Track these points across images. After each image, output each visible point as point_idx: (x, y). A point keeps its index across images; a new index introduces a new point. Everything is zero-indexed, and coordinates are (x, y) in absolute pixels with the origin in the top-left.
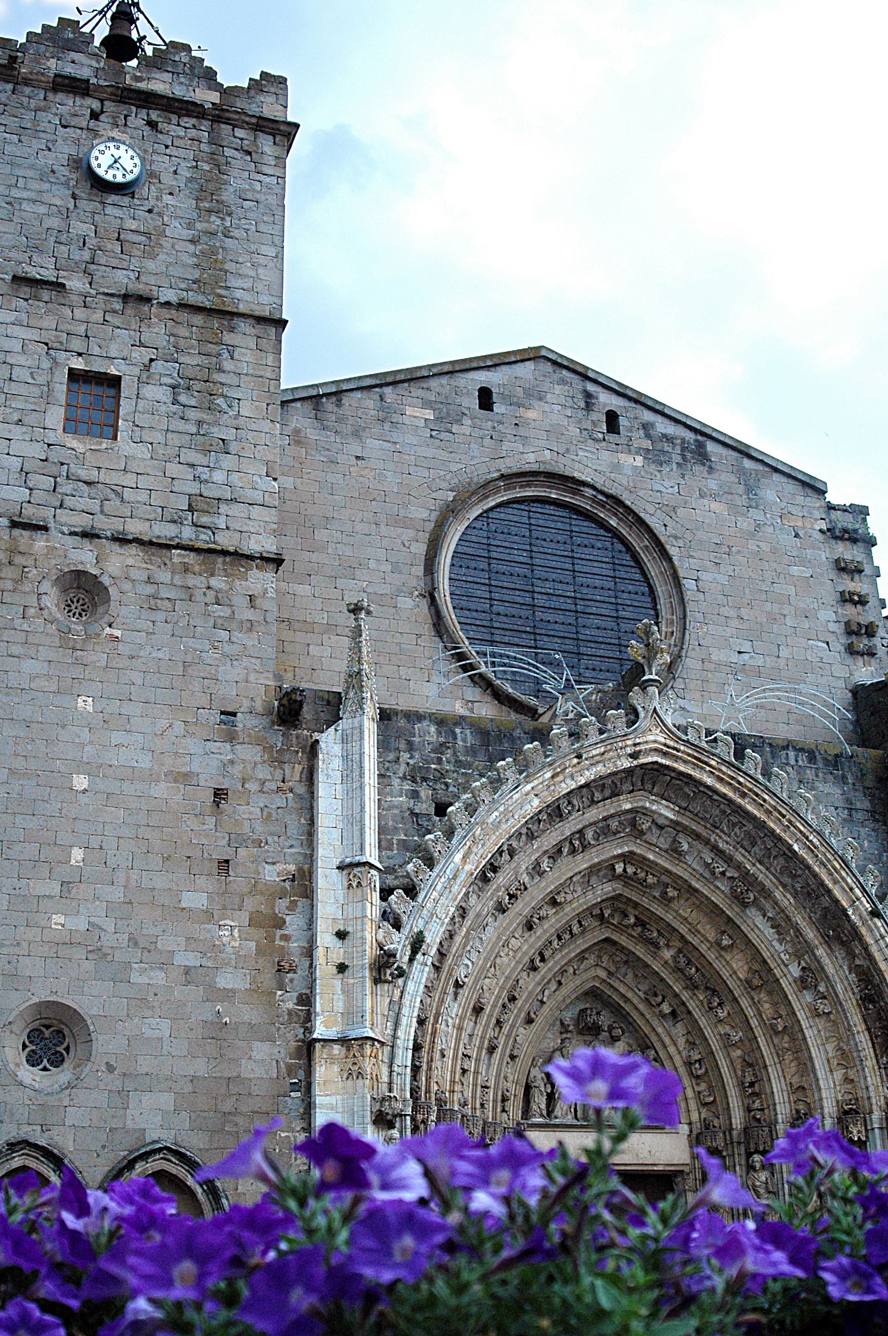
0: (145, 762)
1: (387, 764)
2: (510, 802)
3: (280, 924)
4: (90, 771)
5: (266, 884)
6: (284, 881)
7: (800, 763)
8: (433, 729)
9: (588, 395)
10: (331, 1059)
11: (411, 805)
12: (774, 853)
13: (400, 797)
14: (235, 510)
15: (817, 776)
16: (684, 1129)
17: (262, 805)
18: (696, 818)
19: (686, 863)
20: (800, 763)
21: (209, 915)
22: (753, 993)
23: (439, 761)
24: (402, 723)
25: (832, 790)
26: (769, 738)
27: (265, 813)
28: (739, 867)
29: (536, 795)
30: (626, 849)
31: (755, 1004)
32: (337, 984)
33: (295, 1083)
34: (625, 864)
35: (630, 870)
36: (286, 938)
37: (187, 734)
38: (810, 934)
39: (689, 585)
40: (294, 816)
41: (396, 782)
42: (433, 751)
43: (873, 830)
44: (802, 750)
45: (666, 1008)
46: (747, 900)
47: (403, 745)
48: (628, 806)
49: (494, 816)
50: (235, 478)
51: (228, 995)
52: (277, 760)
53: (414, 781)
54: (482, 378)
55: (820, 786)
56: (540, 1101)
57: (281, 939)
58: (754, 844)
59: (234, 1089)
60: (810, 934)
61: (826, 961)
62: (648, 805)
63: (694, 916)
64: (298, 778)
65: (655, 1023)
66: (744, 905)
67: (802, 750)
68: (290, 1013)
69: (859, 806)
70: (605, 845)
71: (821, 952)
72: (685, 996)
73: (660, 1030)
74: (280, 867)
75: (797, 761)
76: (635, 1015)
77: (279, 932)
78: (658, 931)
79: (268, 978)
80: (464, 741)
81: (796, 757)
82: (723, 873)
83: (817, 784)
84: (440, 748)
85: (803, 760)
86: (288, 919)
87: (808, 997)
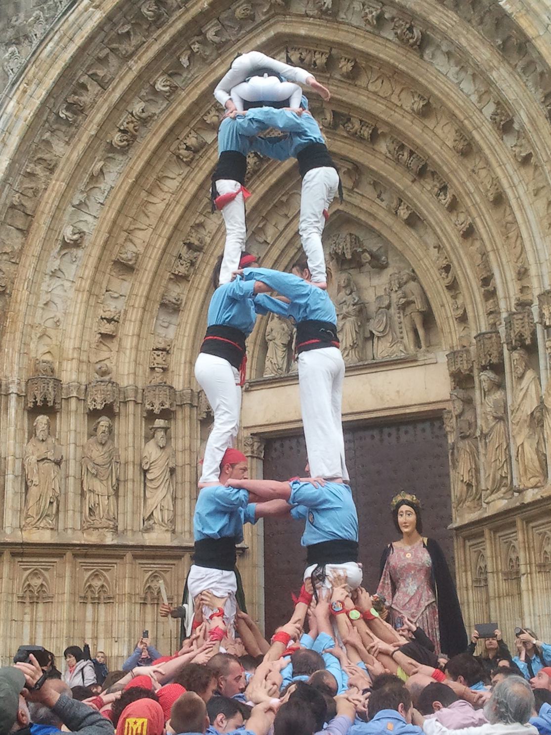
2: (66, 26)
19: (344, 23)
22: (466, 161)
29: (97, 7)
30: (272, 33)
34: (287, 52)
45: (404, 213)
49: (48, 48)
70: (247, 38)
78: (361, 121)
82: (380, 18)
87: (510, 141)
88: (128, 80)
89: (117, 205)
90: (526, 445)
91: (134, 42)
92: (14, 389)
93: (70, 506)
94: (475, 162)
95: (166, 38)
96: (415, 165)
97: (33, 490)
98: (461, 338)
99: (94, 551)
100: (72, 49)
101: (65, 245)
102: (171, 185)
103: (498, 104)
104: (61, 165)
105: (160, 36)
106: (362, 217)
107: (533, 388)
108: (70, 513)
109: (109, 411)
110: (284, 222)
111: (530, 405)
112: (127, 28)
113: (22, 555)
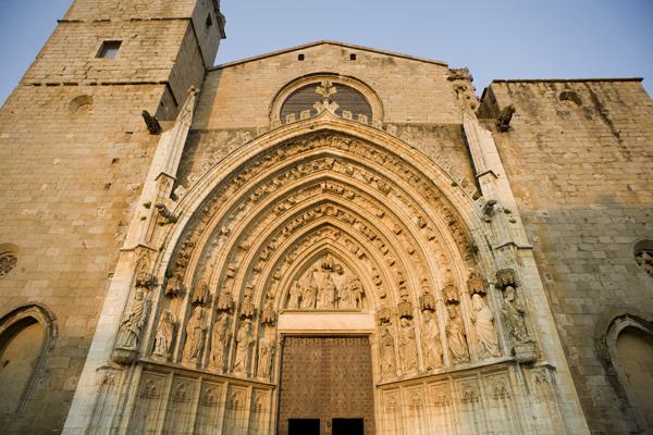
0: (87, 151)
4: (62, 157)
9: (343, 51)
10: (127, 259)
12: (394, 162)
14: (155, 71)
16: (374, 312)
21: (95, 205)
28: (380, 174)
31: (400, 242)
32: (140, 226)
35: (329, 186)
37: (109, 141)
38: (419, 198)
39: (385, 101)
45: (360, 253)
47: (211, 140)
48: (317, 153)
50: (157, 63)
51: (92, 236)
52: (145, 146)
54: (300, 52)
56: (294, 300)
58: (384, 161)
59: (81, 277)
60: (419, 198)
61: (431, 212)
62: (328, 151)
63: (365, 205)
65: (357, 261)
66: (387, 192)
71: (426, 206)
72: (367, 245)
73: (360, 265)
76: (347, 259)
79: (114, 228)
82: (372, 179)
87: (424, 231)
88: (265, 176)
89: (246, 223)
90: (434, 350)
91: (271, 163)
92: (188, 291)
93: (205, 353)
94: (401, 237)
95: (284, 165)
96: (371, 236)
97: (189, 342)
98: (382, 306)
99: (213, 378)
100: (247, 157)
101: (221, 233)
102: (267, 221)
103: (420, 218)
106: (337, 252)
107: (435, 327)
108: (204, 358)
109: (227, 311)
110: (304, 248)
111: (435, 333)
113: (179, 375)
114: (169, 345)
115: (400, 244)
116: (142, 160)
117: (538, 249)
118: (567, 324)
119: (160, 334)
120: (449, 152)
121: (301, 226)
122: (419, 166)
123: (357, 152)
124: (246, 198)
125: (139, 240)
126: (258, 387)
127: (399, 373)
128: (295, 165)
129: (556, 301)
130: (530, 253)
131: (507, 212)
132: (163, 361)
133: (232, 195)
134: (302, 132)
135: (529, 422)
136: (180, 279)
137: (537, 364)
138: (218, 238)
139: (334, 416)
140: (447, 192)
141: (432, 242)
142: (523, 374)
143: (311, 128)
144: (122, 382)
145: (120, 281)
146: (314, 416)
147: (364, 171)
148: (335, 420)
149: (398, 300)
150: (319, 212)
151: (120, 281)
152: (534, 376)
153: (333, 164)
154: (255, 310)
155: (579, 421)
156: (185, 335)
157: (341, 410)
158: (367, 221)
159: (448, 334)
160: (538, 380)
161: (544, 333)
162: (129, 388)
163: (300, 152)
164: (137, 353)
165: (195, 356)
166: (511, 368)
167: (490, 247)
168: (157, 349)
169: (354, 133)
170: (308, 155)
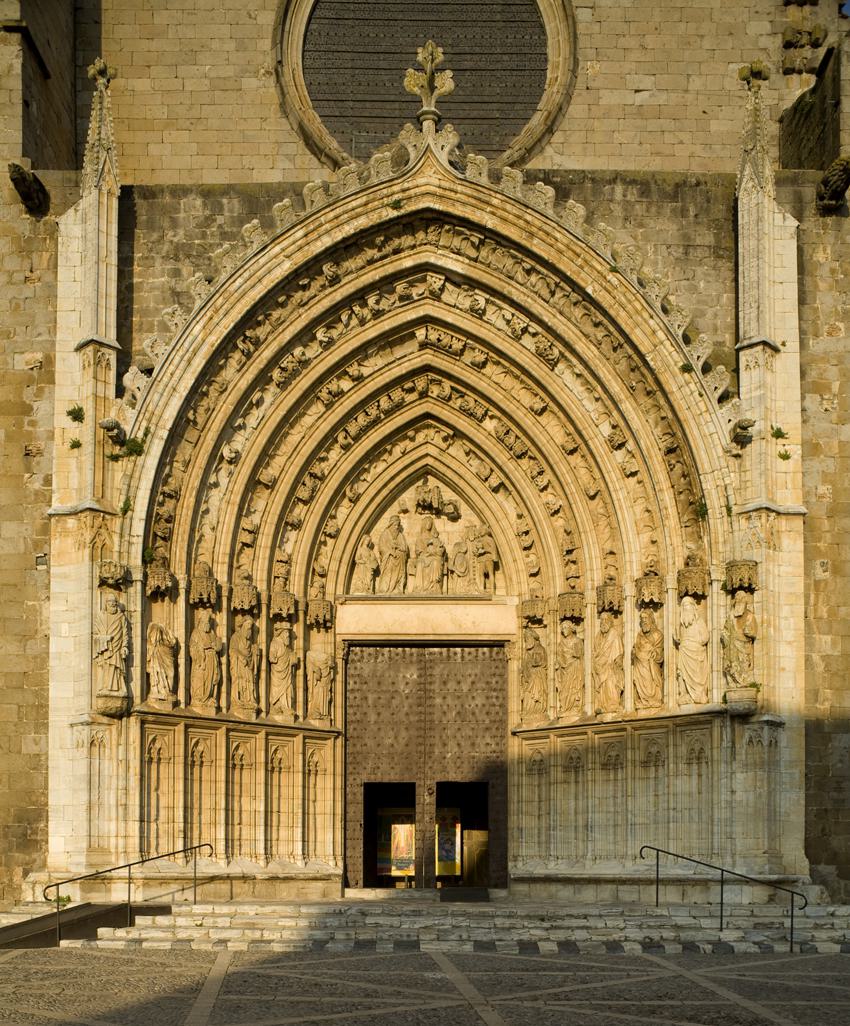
1: (150, 245)
3: (28, 410)
5: (14, 374)
6: (32, 369)
7: (629, 198)
8: (199, 202)
10: (65, 532)
11: (173, 283)
13: (163, 276)
15: (647, 211)
17: (10, 297)
18: (488, 270)
20: (629, 198)
23: (204, 236)
24: (168, 199)
25: (667, 227)
26: (593, 172)
27: (13, 305)
32: (73, 462)
33: (41, 557)
36: (33, 423)
38: (616, 387)
40: (41, 306)
41: (158, 262)
42: (198, 226)
43: (714, 268)
44: (633, 182)
46: (550, 357)
47: (166, 223)
48: (408, 263)
53: (177, 259)
55: (652, 224)
57: (28, 425)
62: (432, 260)
64: (45, 264)
67: (633, 182)
68: (37, 493)
69: (698, 242)
71: (627, 406)
74: (28, 356)
75: (625, 196)
77: (26, 419)
80: (231, 211)
81: (625, 190)
83: (647, 221)
84: (209, 221)
85: (633, 194)
86: (35, 406)
87: (620, 455)
91: (308, 294)
104: (229, 389)
105: (331, 293)
112: (306, 281)
114: (171, 682)
115: (574, 473)
116: (28, 290)
117: (820, 512)
118: (829, 653)
119: (153, 668)
120: (700, 263)
121: (376, 422)
122: (622, 319)
123: (495, 266)
124: (262, 380)
125: (79, 490)
126: (313, 735)
127: (552, 715)
128: (360, 296)
129: (823, 611)
130: (798, 523)
131: (779, 434)
132: (167, 708)
133: (236, 377)
134: (374, 219)
135: (725, 796)
136: (166, 563)
137: (754, 719)
138: (217, 470)
139: (440, 778)
140: (671, 386)
141: (633, 480)
142: (733, 730)
143: (396, 205)
144: (114, 742)
145: (65, 577)
146: (407, 779)
147: (508, 311)
148: (440, 785)
149: (560, 586)
150: (411, 390)
151: (65, 577)
152: (747, 736)
153: (444, 285)
154: (296, 603)
155: (794, 796)
156: (189, 661)
157: (451, 767)
158: (511, 418)
159: (635, 660)
160: (751, 741)
161: (784, 669)
162: (127, 750)
163: (371, 262)
164: (129, 698)
165: (211, 695)
166: (717, 722)
167: (729, 510)
168: (154, 689)
169: (490, 222)
170: (390, 269)
